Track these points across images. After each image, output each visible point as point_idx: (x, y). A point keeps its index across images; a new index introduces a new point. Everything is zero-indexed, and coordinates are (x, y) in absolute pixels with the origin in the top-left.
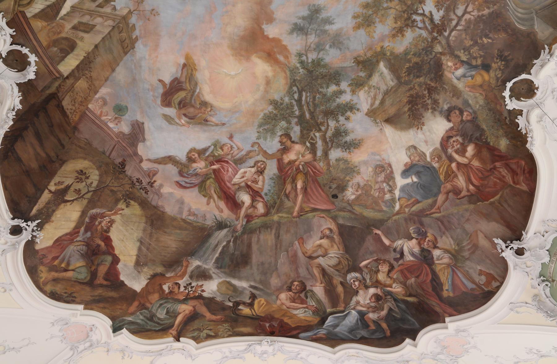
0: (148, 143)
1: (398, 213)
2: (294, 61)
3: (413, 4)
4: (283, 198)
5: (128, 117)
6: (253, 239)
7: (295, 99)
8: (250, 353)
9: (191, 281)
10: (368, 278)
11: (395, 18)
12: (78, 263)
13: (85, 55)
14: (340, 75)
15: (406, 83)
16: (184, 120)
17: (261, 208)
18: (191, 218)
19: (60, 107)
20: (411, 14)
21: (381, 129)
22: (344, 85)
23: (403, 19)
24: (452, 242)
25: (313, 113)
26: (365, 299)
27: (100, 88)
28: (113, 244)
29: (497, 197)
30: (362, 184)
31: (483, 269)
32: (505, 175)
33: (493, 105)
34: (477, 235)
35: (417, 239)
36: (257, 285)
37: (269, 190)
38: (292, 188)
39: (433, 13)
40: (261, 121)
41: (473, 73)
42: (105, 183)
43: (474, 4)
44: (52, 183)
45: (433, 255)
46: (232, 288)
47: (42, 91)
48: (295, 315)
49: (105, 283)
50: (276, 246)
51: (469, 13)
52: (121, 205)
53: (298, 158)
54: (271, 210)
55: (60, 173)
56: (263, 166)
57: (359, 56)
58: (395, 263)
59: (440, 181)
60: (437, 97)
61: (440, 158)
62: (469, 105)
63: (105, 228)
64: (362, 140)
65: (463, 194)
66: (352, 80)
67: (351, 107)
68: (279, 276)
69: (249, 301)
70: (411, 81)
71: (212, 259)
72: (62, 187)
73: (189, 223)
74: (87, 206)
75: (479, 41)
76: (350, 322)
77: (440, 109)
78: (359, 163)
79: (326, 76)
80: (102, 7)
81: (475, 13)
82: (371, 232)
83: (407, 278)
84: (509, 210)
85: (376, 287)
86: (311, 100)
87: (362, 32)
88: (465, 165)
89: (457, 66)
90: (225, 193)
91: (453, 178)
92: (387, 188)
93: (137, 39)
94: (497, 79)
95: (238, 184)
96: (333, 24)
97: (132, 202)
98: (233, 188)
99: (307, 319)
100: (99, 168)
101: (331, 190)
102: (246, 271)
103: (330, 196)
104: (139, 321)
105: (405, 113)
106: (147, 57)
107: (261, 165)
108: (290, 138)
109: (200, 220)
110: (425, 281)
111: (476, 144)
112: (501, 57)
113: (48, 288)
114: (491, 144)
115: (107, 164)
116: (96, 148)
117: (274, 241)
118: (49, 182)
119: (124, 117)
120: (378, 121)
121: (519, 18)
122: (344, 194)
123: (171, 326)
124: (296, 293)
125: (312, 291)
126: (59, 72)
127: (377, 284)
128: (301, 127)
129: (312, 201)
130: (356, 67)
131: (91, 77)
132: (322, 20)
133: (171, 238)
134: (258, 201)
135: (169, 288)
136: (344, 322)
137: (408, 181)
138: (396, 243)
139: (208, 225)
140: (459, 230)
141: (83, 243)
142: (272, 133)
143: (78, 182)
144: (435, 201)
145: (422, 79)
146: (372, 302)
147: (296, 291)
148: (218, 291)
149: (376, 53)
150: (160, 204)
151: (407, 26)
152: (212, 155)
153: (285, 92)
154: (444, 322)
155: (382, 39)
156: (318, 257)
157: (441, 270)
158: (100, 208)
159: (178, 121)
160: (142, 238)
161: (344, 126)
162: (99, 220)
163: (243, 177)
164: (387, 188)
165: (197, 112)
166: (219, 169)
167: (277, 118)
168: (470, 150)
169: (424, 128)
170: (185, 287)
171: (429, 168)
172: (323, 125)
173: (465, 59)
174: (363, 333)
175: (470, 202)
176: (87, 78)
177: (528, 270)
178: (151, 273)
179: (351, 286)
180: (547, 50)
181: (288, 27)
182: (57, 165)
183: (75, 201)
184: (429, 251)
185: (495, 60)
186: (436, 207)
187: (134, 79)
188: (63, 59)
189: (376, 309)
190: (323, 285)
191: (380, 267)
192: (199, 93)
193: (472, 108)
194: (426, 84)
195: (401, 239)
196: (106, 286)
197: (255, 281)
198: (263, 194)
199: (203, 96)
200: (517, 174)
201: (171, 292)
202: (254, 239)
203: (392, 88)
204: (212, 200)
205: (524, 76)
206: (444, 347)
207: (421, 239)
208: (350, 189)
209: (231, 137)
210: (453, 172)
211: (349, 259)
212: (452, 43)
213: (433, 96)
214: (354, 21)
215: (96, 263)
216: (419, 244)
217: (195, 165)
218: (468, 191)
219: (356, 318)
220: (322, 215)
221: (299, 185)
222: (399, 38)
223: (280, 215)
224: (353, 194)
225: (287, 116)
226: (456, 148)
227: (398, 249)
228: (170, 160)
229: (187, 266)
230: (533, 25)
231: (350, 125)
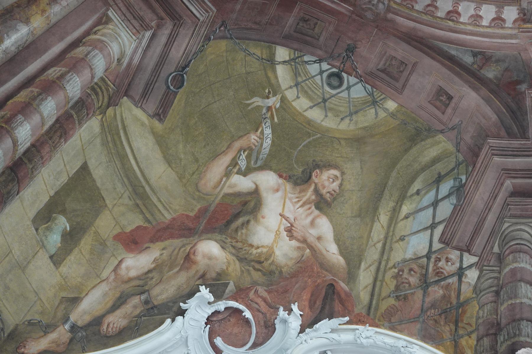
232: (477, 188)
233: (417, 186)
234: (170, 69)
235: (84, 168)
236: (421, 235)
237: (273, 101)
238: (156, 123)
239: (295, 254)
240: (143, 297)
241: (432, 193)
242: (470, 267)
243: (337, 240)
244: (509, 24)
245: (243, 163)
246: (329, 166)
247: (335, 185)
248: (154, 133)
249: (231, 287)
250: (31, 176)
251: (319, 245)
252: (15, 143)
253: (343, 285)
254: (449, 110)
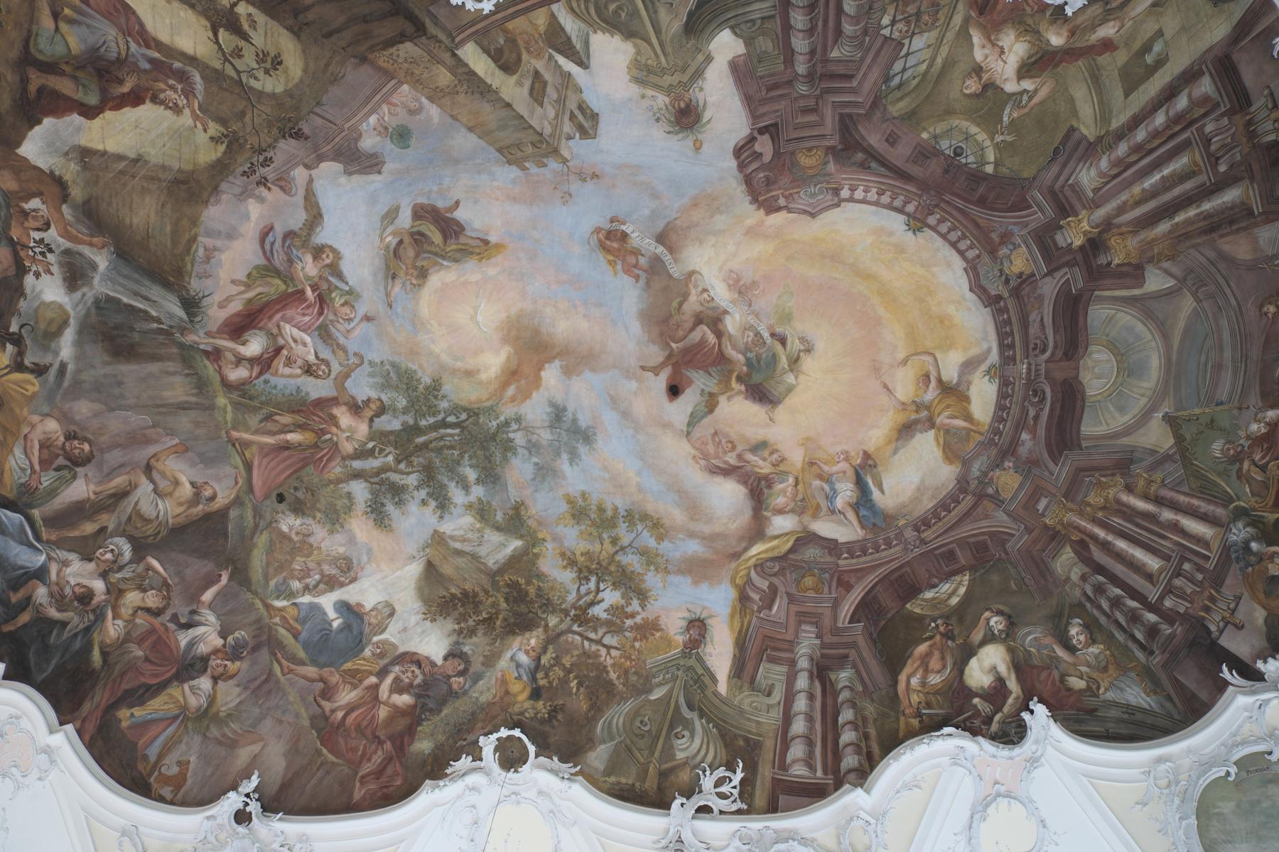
0: (343, 179)
1: (268, 607)
2: (507, 412)
3: (610, 573)
4: (264, 411)
5: (389, 148)
6: (171, 364)
7: (445, 418)
10: (126, 574)
11: (588, 552)
12: (75, 41)
13: (494, 87)
14: (494, 483)
15: (494, 583)
16: (391, 240)
17: (237, 374)
18: (201, 252)
19: (401, 38)
20: (597, 574)
21: (414, 557)
22: (478, 491)
23: (588, 563)
24: (232, 705)
25: (427, 448)
26: (75, 575)
27: (439, 106)
28: (126, 110)
29: (331, 757)
30: (311, 540)
31: (191, 767)
32: (373, 761)
33: (481, 716)
34: (254, 743)
35: (224, 646)
36: (68, 376)
37: (275, 387)
38: (286, 426)
39: (601, 604)
40: (403, 366)
41: (525, 678)
42: (259, 102)
43: (620, 658)
44: (251, 9)
46: (53, 328)
47: (429, 12)
48: (11, 451)
49: (32, 88)
50: (163, 406)
51: (609, 653)
52: (214, 128)
53: (343, 431)
54: (237, 393)
55: (273, 24)
56: (321, 373)
57: (526, 508)
59: (342, 664)
60: (480, 633)
61: (382, 655)
62: (475, 682)
64: (392, 531)
65: (323, 703)
66: (489, 503)
67: (443, 505)
68: (96, 415)
69: (27, 362)
70: (498, 590)
71: (115, 291)
72: (246, 27)
73: (188, 250)
74: (207, 66)
75: (571, 676)
76: (17, 555)
77: (461, 640)
78: (351, 530)
79: (490, 462)
80: (570, 119)
81: (609, 661)
82: (221, 566)
83: (140, 642)
84: (314, 781)
85: (108, 592)
86: (448, 443)
87: (564, 507)
88: (376, 698)
89: (532, 653)
90: (260, 311)
91: (349, 683)
92: (311, 581)
93: (524, 169)
94: (522, 714)
95: (280, 334)
96: (571, 465)
97: (222, 148)
98: (271, 325)
99: (6, 475)
100: (289, 93)
101: (292, 491)
102: (97, 353)
103: (280, 490)
105: (447, 589)
106: (495, 184)
107: (323, 371)
108: (378, 415)
109: (198, 268)
110: (143, 674)
111: (415, 706)
112: (554, 711)
114: (420, 728)
115: (297, 109)
116: (327, 92)
117: (171, 401)
118: (253, 4)
119: (389, 142)
120: (428, 550)
121: (610, 723)
122: (287, 513)
125: (74, 477)
126: (463, 42)
128: (400, 431)
129: (266, 461)
130: (509, 506)
131: (457, 93)
132: (575, 448)
133: (153, 217)
134: (252, 369)
135: (34, 210)
136: (12, 543)
137: (332, 614)
138: (208, 612)
139: (189, 283)
140: (257, 711)
141: (124, 54)
142: (383, 385)
143: (257, 55)
144: (302, 663)
145: (504, 605)
146: (72, 588)
148: (43, 303)
149: (535, 532)
150: (224, 197)
151: (580, 571)
152: (332, 287)
153: (457, 401)
154: (61, 724)
155: (556, 539)
156: (152, 481)
157: (171, 696)
158: (205, 89)
159: (389, 230)
160: (146, 162)
161: (410, 499)
162: (180, 87)
163: (295, 341)
164: (311, 581)
165: (409, 262)
166: (306, 300)
167: (410, 391)
168: (405, 699)
169: (428, 623)
170: (42, 240)
171: (358, 644)
172: (407, 466)
173: (543, 662)
175: (313, 718)
176: (456, 86)
178: (67, 177)
179: (100, 548)
180: (573, 771)
181: (559, 399)
182: (290, 22)
183: (216, 47)
184: (205, 670)
185: (548, 704)
186: (293, 667)
187: (457, 162)
188: (486, 51)
191: (153, 591)
192: (442, 265)
193: (471, 687)
194: (497, 613)
195: (218, 619)
196: (24, 90)
197: (78, 371)
198: (266, 376)
199: (437, 272)
200: (378, 779)
201: (25, 214)
202: (171, 366)
203: (484, 564)
204: (242, 288)
205: (532, 749)
207: (226, 653)
208: (298, 522)
209: (367, 318)
210: (361, 681)
211: (159, 537)
212: (563, 638)
213: (481, 627)
214: (577, 495)
215: (80, 74)
216: (216, 652)
217: (309, 258)
218: (333, 711)
219: (29, 565)
220: (240, 481)
221: (293, 437)
222: (561, 563)
223: (229, 408)
224: (291, 528)
225: (417, 407)
226: (403, 677)
227: (197, 618)
228: (315, 217)
229: (91, 244)
230: (604, 742)
231: (413, 507)
232: (875, 83)
233: (915, 82)
234: (1061, 160)
235: (1127, 95)
236: (916, 49)
237: (999, 138)
238: (1075, 124)
239: (1002, 36)
240: (1109, 7)
241: (905, 77)
242: (886, 27)
243: (972, 45)
244: (846, 187)
245: (1025, 98)
246: (970, 96)
247: (968, 83)
248: (1078, 118)
249: (1048, 13)
250: (1163, 90)
251: (984, 42)
252: (1167, 112)
253: (973, 15)
254: (888, 132)
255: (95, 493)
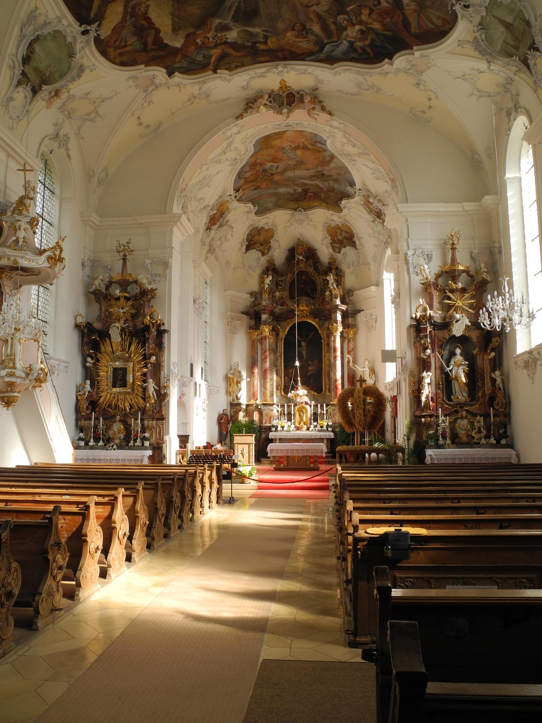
8: (270, 73)
9: (216, 34)
12: (132, 40)
28: (153, 21)
45: (403, 3)
49: (154, 47)
58: (374, 8)
63: (144, 12)
69: (263, 41)
71: (229, 16)
85: (361, 24)
104: (185, 66)
113: (118, 60)
123: (209, 64)
124: (298, 32)
125: (311, 29)
127: (361, 22)
135: (201, 41)
136: (338, 49)
147: (298, 30)
154: (412, 49)
156: (312, 6)
170: (212, 38)
174: (354, 55)
177: (471, 19)
178: (186, 33)
179: (341, 24)
189: (361, 40)
190: (319, 25)
191: (362, 11)
201: (203, 43)
206: (413, 65)
219: (347, 46)
229: (211, 24)
255: (318, 23)
